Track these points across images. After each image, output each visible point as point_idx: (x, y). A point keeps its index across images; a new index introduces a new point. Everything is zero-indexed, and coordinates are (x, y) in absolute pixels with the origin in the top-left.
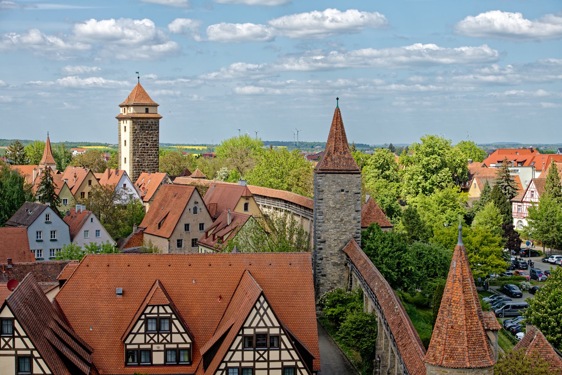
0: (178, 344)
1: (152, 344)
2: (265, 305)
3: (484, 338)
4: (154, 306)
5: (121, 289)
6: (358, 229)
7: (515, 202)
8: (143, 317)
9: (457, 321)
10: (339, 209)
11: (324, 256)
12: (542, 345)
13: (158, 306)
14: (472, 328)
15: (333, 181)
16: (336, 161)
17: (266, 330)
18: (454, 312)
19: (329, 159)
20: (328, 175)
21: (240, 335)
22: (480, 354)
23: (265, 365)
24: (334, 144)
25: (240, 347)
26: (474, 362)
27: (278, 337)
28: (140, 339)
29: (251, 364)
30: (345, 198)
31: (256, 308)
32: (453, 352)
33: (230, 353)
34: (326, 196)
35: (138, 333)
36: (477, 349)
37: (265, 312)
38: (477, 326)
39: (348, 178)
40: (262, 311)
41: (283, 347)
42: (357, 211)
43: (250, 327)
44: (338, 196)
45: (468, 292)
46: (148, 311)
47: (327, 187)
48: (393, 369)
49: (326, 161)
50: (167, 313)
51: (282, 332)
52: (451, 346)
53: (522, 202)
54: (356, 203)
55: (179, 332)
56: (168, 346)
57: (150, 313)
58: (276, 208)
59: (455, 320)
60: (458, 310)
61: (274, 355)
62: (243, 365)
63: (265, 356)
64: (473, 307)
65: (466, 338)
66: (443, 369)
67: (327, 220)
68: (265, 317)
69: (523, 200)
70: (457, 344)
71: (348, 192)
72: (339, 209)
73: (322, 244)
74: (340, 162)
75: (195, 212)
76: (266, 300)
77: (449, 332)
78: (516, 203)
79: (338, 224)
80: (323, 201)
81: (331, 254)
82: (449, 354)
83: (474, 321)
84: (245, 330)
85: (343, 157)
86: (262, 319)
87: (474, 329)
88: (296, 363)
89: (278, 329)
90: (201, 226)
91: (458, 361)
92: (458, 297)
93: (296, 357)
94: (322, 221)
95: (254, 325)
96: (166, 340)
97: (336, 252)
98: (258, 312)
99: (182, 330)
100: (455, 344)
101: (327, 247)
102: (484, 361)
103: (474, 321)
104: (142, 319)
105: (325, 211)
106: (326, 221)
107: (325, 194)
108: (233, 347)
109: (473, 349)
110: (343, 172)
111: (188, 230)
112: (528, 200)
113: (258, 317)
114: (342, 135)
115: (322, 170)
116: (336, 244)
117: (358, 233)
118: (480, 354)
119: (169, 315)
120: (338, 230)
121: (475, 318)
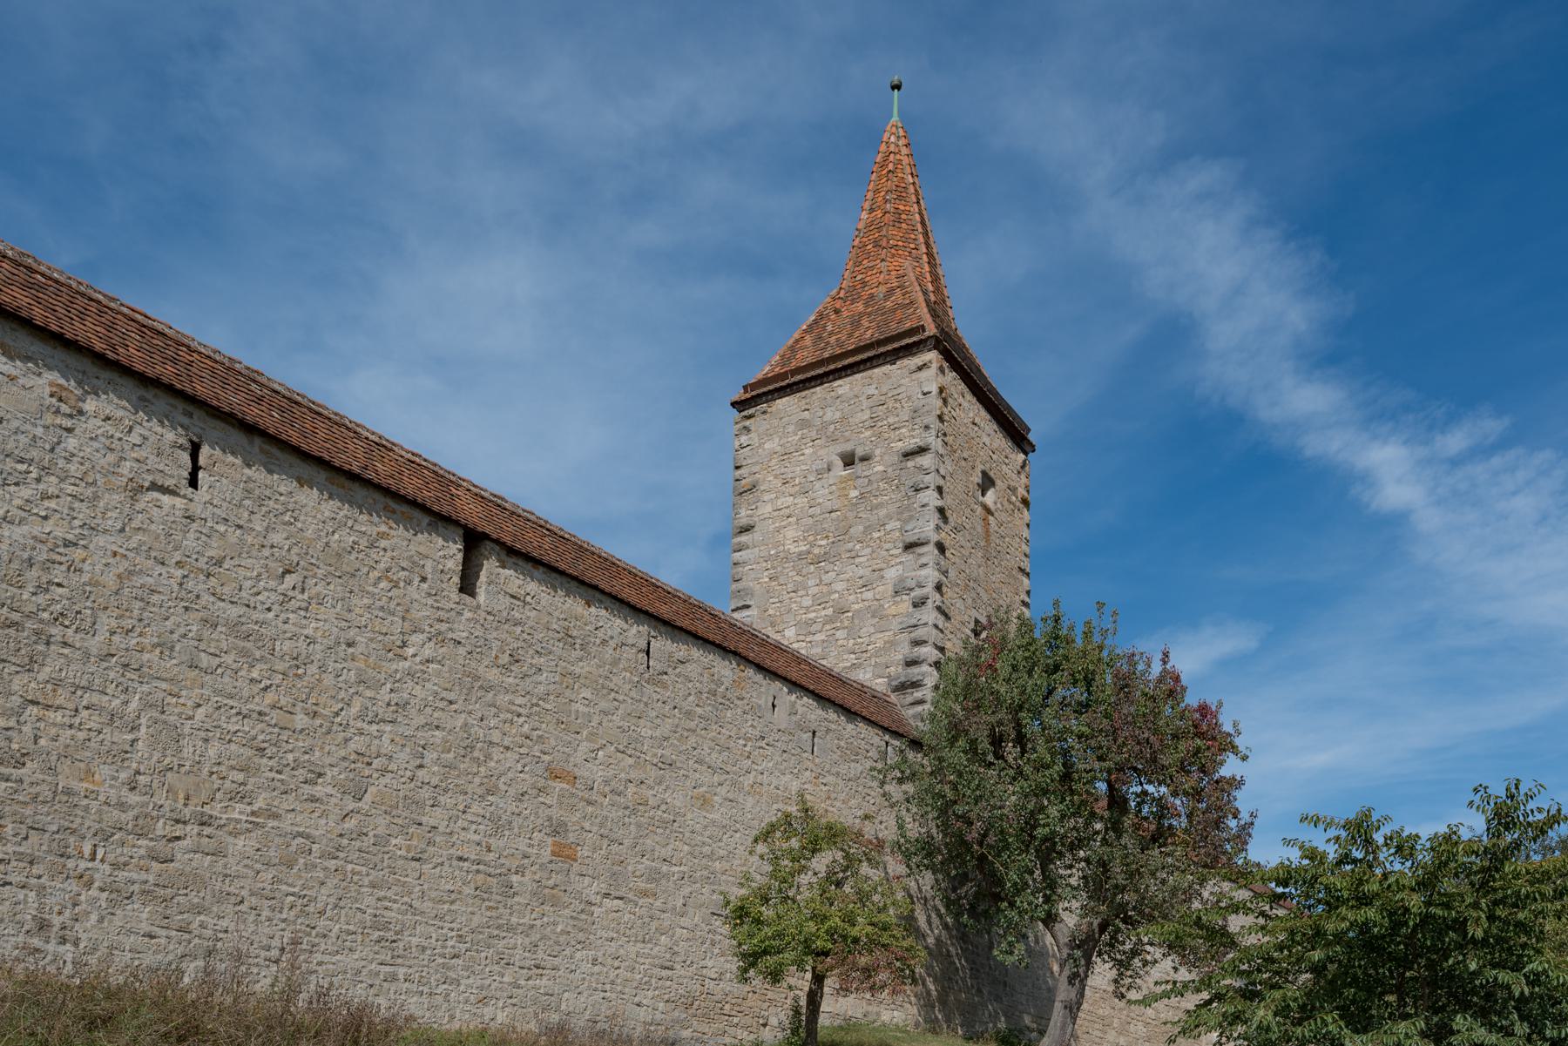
6: (917, 643)
15: (804, 424)
19: (808, 340)
20: (782, 403)
34: (769, 508)
39: (872, 390)
42: (909, 547)
44: (821, 492)
47: (773, 462)
54: (908, 508)
71: (864, 459)
74: (850, 335)
79: (820, 637)
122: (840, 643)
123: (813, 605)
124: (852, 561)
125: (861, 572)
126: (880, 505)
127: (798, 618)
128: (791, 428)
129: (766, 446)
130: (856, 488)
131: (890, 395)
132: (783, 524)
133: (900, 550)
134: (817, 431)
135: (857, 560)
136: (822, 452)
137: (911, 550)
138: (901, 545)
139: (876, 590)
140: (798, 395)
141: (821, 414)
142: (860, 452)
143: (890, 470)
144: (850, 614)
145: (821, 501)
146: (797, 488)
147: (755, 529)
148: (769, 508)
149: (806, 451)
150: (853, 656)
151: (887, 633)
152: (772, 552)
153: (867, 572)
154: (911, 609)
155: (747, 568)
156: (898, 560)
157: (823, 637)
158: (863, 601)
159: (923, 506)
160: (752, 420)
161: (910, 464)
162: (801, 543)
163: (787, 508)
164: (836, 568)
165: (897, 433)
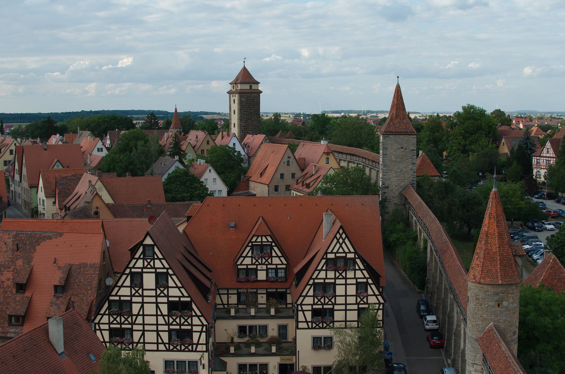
0: (277, 265)
1: (257, 265)
2: (344, 236)
3: (513, 261)
4: (258, 236)
5: (234, 223)
6: (414, 178)
7: (535, 156)
8: (250, 244)
9: (492, 248)
10: (399, 162)
12: (557, 267)
13: (262, 236)
14: (503, 254)
16: (397, 125)
17: (344, 255)
18: (489, 242)
19: (391, 124)
20: (391, 136)
21: (324, 259)
22: (510, 274)
23: (343, 281)
24: (395, 112)
25: (324, 268)
26: (505, 280)
27: (353, 260)
28: (248, 261)
29: (333, 281)
31: (337, 238)
32: (489, 272)
33: (317, 272)
34: (389, 152)
35: (246, 256)
36: (507, 270)
37: (344, 241)
38: (507, 252)
39: (406, 139)
40: (341, 241)
41: (357, 268)
43: (332, 252)
44: (398, 152)
45: (501, 227)
46: (254, 240)
47: (390, 145)
48: (441, 285)
49: (390, 125)
50: (268, 241)
51: (357, 257)
52: (487, 268)
53: (540, 156)
55: (278, 256)
56: (269, 266)
57: (256, 242)
58: (350, 161)
59: (490, 248)
60: (492, 240)
61: (350, 274)
62: (327, 281)
63: (344, 274)
64: (504, 238)
65: (498, 262)
66: (481, 286)
68: (344, 245)
69: (541, 155)
70: (492, 266)
72: (399, 162)
73: (386, 189)
75: (288, 165)
76: (344, 232)
77: (486, 257)
78: (535, 158)
80: (387, 156)
81: (393, 196)
82: (486, 274)
83: (505, 248)
84: (328, 255)
85: (402, 122)
86: (341, 246)
87: (505, 254)
88: (367, 280)
89: (353, 254)
90: (293, 175)
91: (492, 280)
92: (492, 230)
93: (367, 276)
95: (335, 251)
96: (268, 262)
98: (338, 241)
99: (280, 254)
100: (490, 266)
102: (513, 279)
103: (505, 248)
104: (250, 246)
107: (389, 150)
108: (319, 268)
109: (504, 270)
110: (403, 133)
111: (283, 178)
112: (544, 155)
113: (338, 245)
114: (401, 105)
115: (385, 132)
117: (414, 181)
118: (510, 274)
119: (270, 243)
120: (398, 178)
121: (506, 246)
126: (407, 156)
142: (404, 148)
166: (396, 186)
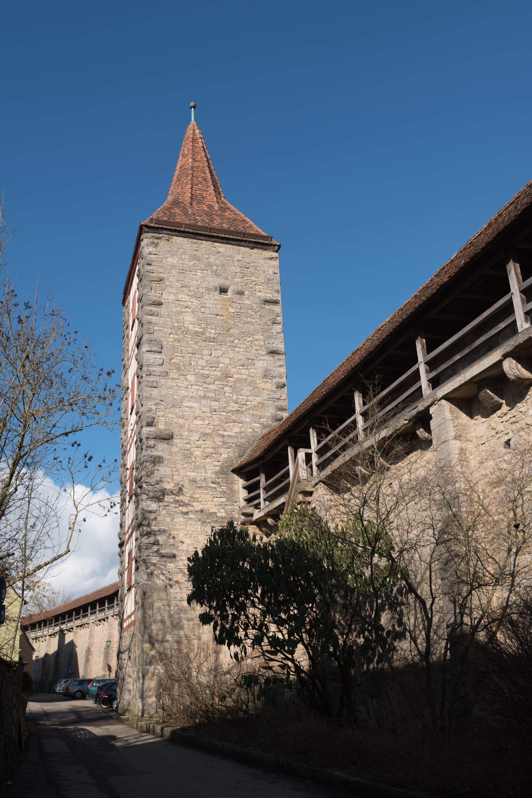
11: (169, 486)
30: (231, 310)
34: (172, 297)
47: (174, 271)
54: (267, 330)
67: (178, 369)
71: (241, 293)
79: (212, 387)
80: (162, 310)
94: (159, 369)
97: (210, 474)
101: (179, 457)
105: (168, 340)
106: (174, 374)
116: (210, 450)
122: (227, 394)
123: (206, 366)
124: (233, 349)
125: (241, 356)
126: (248, 323)
127: (197, 371)
128: (187, 257)
129: (168, 260)
130: (232, 307)
131: (252, 264)
132: (182, 310)
133: (264, 353)
134: (205, 265)
135: (236, 349)
136: (207, 278)
137: (272, 355)
138: (265, 350)
139: (250, 370)
140: (190, 240)
141: (207, 257)
143: (255, 306)
144: (233, 379)
145: (210, 306)
146: (192, 293)
147: (162, 306)
148: (172, 297)
149: (199, 274)
150: (236, 405)
151: (260, 398)
152: (175, 325)
153: (243, 358)
154: (274, 388)
155: (158, 328)
156: (263, 358)
157: (215, 388)
158: (240, 374)
159: (277, 333)
160: (159, 241)
161: (267, 307)
162: (196, 326)
163: (185, 301)
164: (222, 349)
165: (257, 287)
166: (205, 434)
